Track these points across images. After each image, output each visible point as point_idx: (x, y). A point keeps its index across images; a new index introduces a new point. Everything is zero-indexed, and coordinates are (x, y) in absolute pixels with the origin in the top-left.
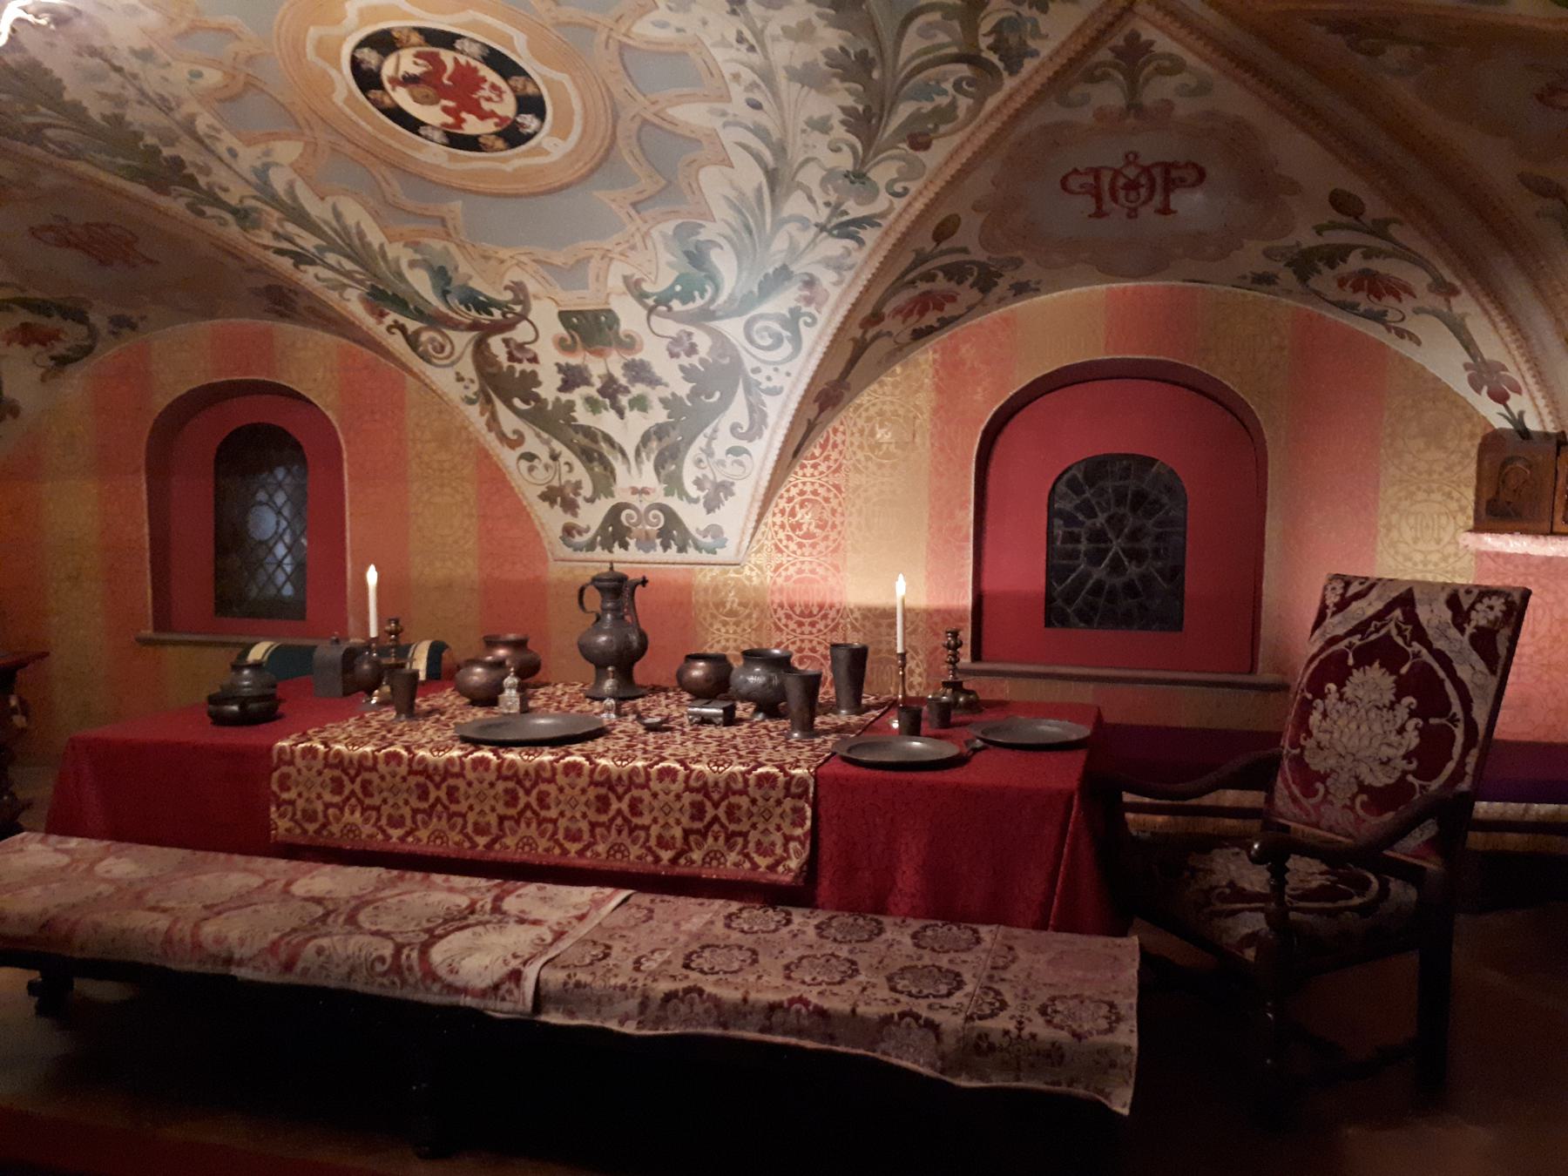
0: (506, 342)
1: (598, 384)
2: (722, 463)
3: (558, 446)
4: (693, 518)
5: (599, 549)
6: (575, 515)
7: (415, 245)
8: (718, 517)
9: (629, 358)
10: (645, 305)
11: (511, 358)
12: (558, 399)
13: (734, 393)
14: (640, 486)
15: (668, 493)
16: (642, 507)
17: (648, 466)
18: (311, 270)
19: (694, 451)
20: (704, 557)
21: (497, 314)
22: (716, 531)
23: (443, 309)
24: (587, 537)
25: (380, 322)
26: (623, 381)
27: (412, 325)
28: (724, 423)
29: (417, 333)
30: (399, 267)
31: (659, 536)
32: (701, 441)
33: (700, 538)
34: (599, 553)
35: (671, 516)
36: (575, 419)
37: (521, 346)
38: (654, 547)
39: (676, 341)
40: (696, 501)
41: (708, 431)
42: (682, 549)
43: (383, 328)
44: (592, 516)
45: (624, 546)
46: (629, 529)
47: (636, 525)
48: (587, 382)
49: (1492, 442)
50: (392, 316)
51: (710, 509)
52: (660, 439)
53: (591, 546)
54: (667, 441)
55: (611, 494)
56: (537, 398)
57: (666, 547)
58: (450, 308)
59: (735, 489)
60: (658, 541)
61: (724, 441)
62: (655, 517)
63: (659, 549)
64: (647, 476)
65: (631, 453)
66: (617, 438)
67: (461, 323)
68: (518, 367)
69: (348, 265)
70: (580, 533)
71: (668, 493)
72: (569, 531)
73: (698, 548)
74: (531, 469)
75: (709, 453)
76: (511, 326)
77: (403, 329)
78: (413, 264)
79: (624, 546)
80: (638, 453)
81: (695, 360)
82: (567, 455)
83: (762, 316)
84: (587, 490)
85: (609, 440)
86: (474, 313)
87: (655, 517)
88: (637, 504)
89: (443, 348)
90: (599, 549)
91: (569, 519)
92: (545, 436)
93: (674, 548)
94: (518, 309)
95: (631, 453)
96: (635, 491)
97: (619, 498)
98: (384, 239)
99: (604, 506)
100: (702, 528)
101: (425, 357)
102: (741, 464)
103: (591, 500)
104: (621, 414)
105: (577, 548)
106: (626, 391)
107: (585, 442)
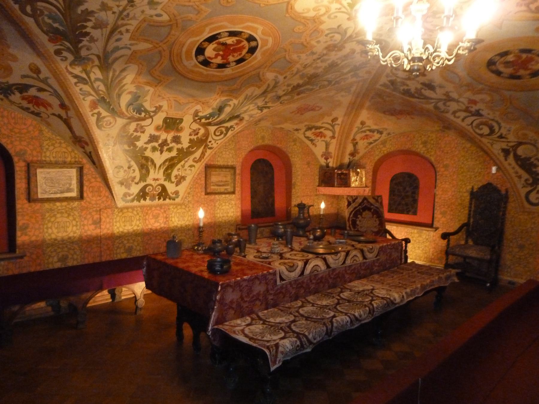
0: (138, 125)
1: (160, 141)
2: (186, 170)
3: (133, 163)
4: (171, 188)
5: (135, 201)
6: (129, 189)
7: (138, 87)
8: (179, 188)
9: (176, 134)
10: (194, 118)
11: (136, 130)
12: (142, 146)
13: (200, 148)
14: (156, 178)
15: (165, 180)
16: (154, 185)
17: (162, 171)
18: (81, 86)
19: (179, 166)
20: (172, 201)
21: (143, 114)
22: (177, 193)
23: (124, 110)
24: (132, 197)
25: (92, 111)
26: (169, 142)
27: (104, 113)
28: (192, 157)
29: (104, 117)
30: (122, 92)
31: (158, 195)
32: (183, 162)
33: (171, 195)
34: (136, 203)
35: (164, 188)
36: (144, 154)
37: (142, 127)
38: (155, 199)
39: (194, 131)
40: (172, 182)
41: (186, 159)
42: (164, 199)
43: (90, 114)
44: (135, 189)
45: (145, 199)
46: (148, 194)
47: (151, 192)
48: (157, 141)
49: (321, 167)
50: (100, 110)
51: (177, 185)
52: (170, 162)
53: (133, 200)
54: (172, 162)
55: (146, 181)
56: (135, 146)
57: (159, 199)
58: (127, 111)
59: (187, 178)
60: (157, 197)
61: (190, 162)
62: (159, 188)
63: (157, 200)
64: (160, 175)
65: (158, 166)
66: (155, 161)
67: (126, 116)
68: (135, 134)
69: (102, 87)
70: (129, 196)
71: (165, 180)
72: (125, 195)
73: (170, 199)
74: (118, 172)
75: (183, 166)
76: (144, 119)
77: (99, 114)
78: (130, 93)
79: (145, 199)
80: (160, 166)
81: (195, 137)
82: (135, 167)
83: (223, 127)
84: (137, 180)
85: (152, 161)
86: (135, 113)
87: (159, 188)
88: (153, 184)
89: (110, 123)
90: (135, 201)
91: (126, 191)
92: (130, 159)
93: (162, 199)
94: (152, 114)
95: (158, 166)
96: (155, 180)
97: (147, 183)
98: (129, 82)
99: (142, 184)
100: (173, 191)
101: (99, 127)
102: (191, 170)
103: (137, 183)
104: (161, 153)
105: (127, 201)
106: (168, 145)
107: (144, 162)
